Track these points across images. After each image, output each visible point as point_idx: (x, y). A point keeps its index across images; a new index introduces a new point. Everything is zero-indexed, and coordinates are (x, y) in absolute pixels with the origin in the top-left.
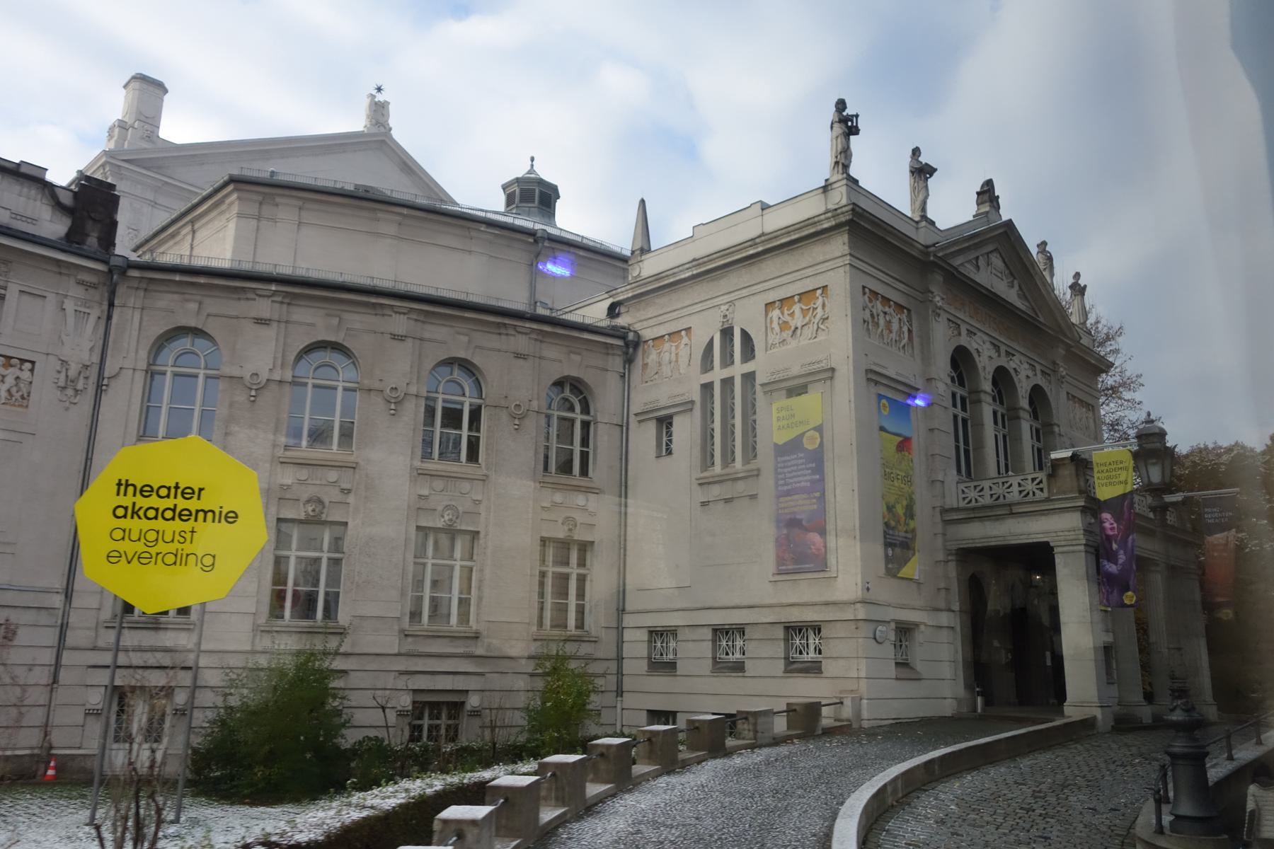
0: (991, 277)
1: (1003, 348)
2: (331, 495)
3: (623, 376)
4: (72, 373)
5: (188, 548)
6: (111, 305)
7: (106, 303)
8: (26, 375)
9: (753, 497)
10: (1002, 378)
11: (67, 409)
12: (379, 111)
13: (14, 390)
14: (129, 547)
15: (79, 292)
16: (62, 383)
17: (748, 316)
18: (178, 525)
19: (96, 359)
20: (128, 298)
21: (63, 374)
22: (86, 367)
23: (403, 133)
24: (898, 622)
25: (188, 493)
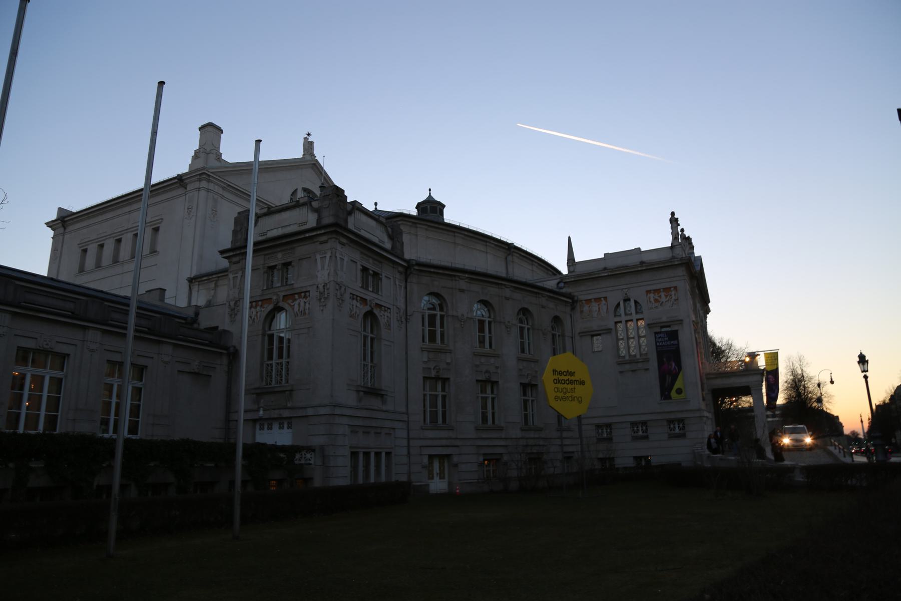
5: (574, 395)
6: (406, 281)
9: (647, 369)
12: (309, 146)
14: (560, 395)
15: (398, 275)
17: (637, 293)
18: (570, 386)
25: (572, 374)
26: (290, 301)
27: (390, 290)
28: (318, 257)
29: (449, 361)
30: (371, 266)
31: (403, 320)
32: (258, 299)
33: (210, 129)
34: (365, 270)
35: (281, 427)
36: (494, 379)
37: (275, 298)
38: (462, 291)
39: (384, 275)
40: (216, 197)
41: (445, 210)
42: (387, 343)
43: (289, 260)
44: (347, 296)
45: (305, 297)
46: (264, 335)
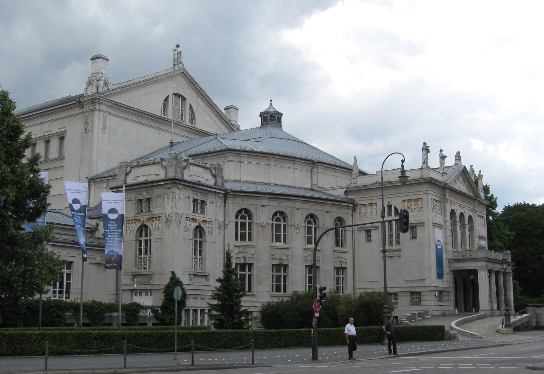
0: (461, 187)
1: (462, 206)
2: (284, 257)
3: (352, 216)
6: (225, 202)
9: (399, 256)
10: (462, 215)
15: (219, 200)
20: (230, 200)
23: (189, 67)
24: (440, 291)
26: (151, 222)
27: (214, 209)
28: (166, 197)
29: (253, 252)
30: (199, 197)
31: (222, 228)
32: (133, 218)
33: (99, 60)
34: (195, 201)
35: (147, 295)
36: (285, 263)
37: (142, 219)
38: (263, 206)
39: (208, 201)
40: (105, 114)
41: (283, 119)
42: (210, 244)
43: (150, 197)
44: (183, 220)
45: (159, 220)
46: (136, 240)
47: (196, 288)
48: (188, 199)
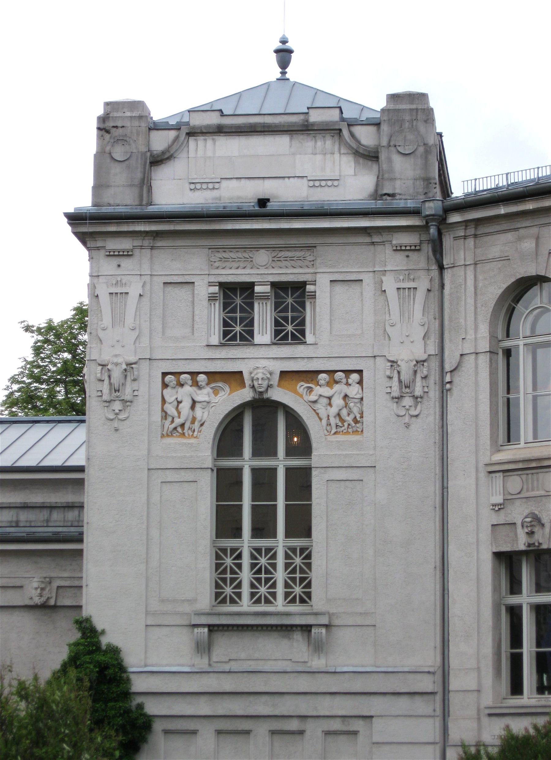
4: (406, 376)
6: (441, 268)
7: (434, 267)
8: (354, 391)
11: (407, 426)
13: (344, 412)
15: (395, 262)
16: (396, 392)
19: (433, 349)
20: (457, 251)
21: (396, 379)
22: (420, 362)
27: (364, 314)
30: (262, 270)
47: (227, 684)
48: (183, 293)
